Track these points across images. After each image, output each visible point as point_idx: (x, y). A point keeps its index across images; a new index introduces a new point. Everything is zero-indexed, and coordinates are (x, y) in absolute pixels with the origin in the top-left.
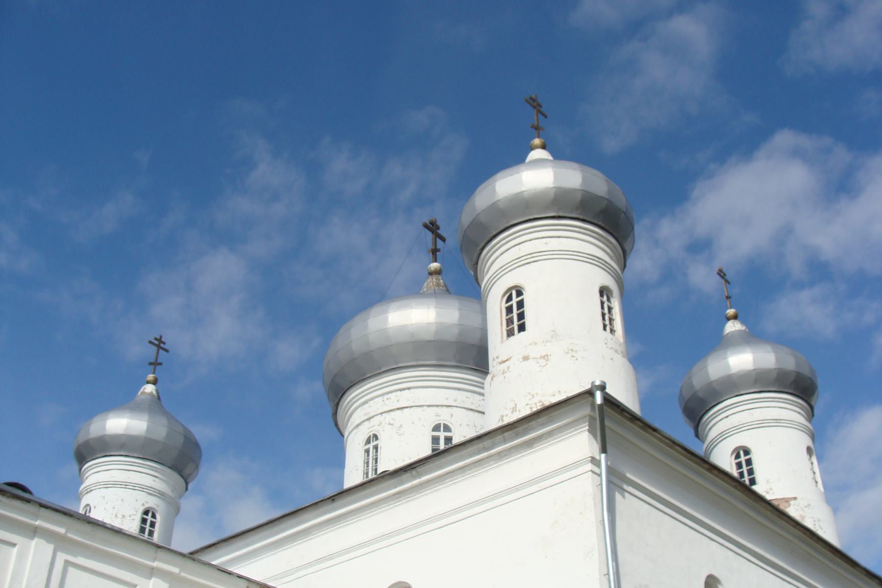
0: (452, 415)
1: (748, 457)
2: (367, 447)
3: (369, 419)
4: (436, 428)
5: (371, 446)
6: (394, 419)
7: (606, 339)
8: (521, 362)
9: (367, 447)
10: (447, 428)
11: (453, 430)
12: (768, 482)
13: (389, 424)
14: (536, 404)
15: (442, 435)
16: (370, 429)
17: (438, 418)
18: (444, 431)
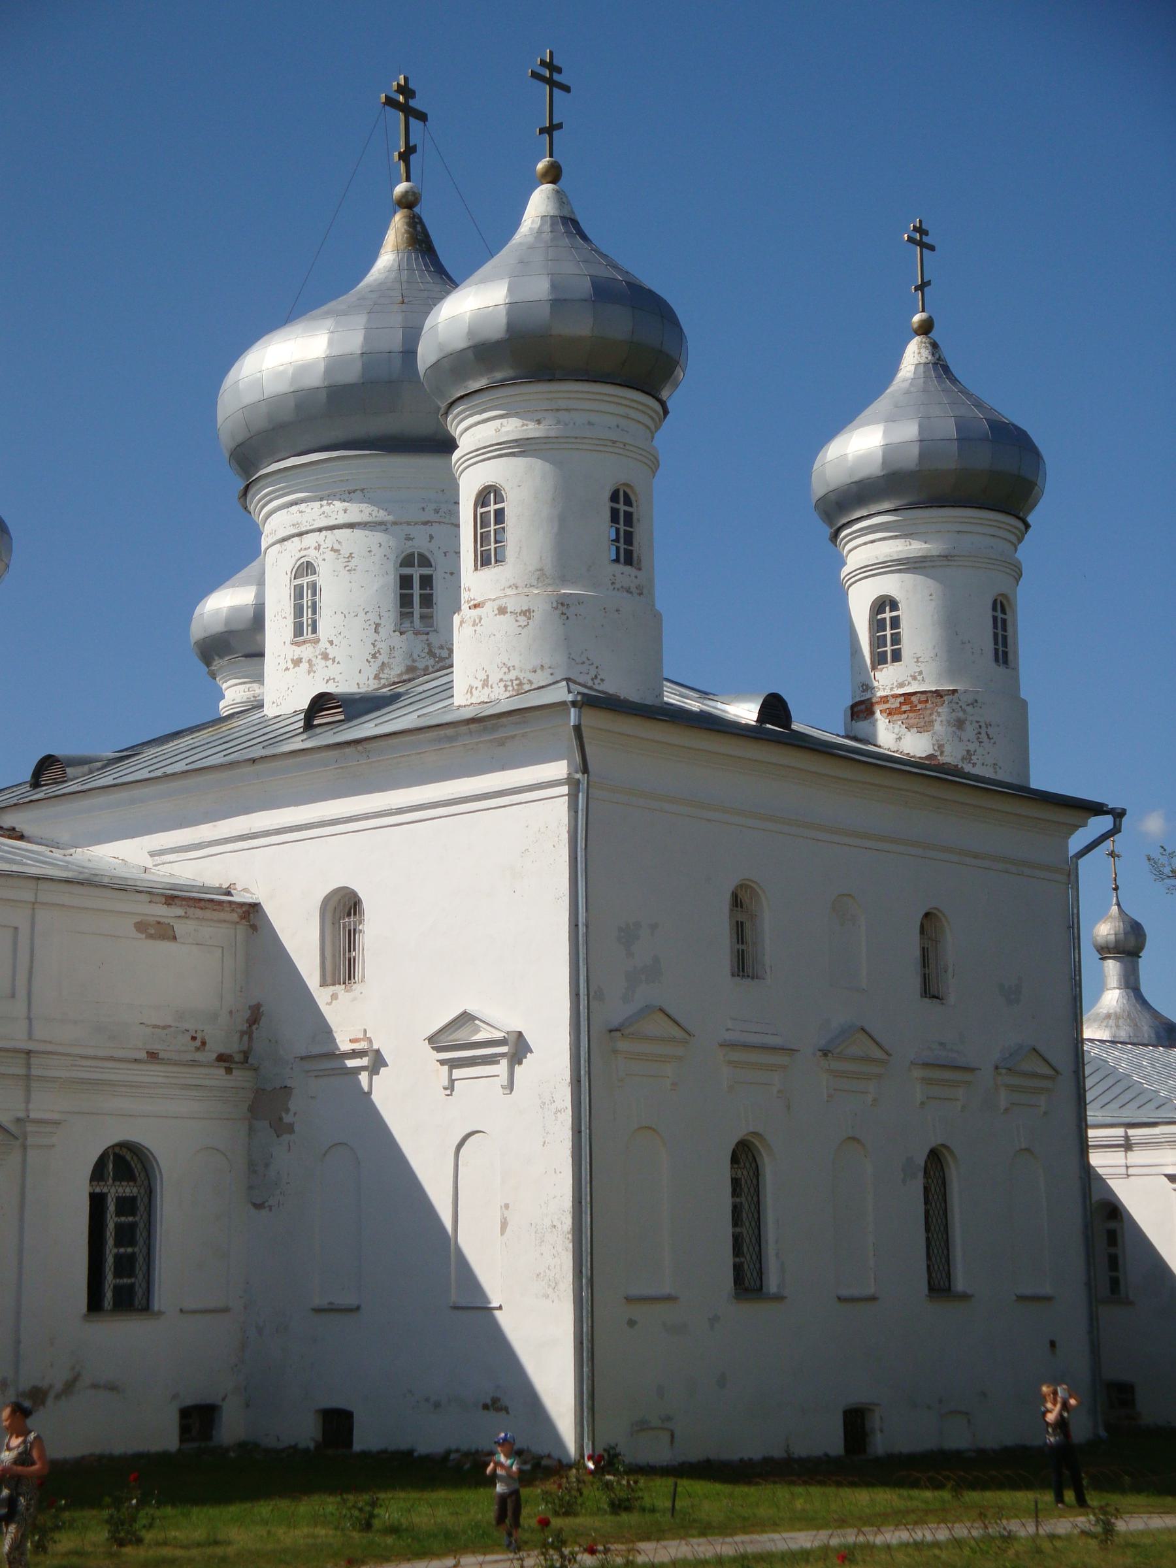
0: (431, 537)
1: (894, 614)
2: (298, 582)
3: (300, 534)
4: (407, 561)
5: (304, 581)
6: (340, 543)
7: (614, 576)
8: (496, 615)
9: (298, 582)
10: (425, 561)
11: (433, 564)
12: (918, 662)
13: (333, 550)
14: (512, 681)
15: (416, 573)
16: (303, 553)
17: (409, 543)
18: (419, 566)
